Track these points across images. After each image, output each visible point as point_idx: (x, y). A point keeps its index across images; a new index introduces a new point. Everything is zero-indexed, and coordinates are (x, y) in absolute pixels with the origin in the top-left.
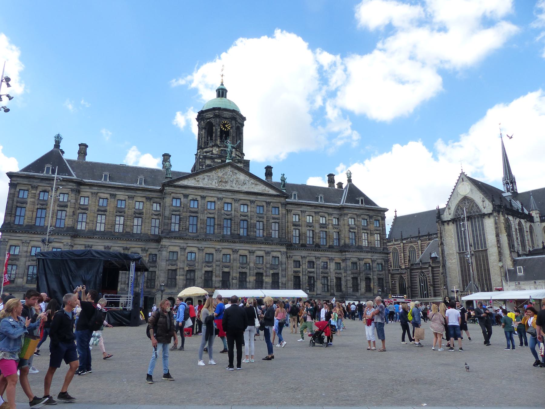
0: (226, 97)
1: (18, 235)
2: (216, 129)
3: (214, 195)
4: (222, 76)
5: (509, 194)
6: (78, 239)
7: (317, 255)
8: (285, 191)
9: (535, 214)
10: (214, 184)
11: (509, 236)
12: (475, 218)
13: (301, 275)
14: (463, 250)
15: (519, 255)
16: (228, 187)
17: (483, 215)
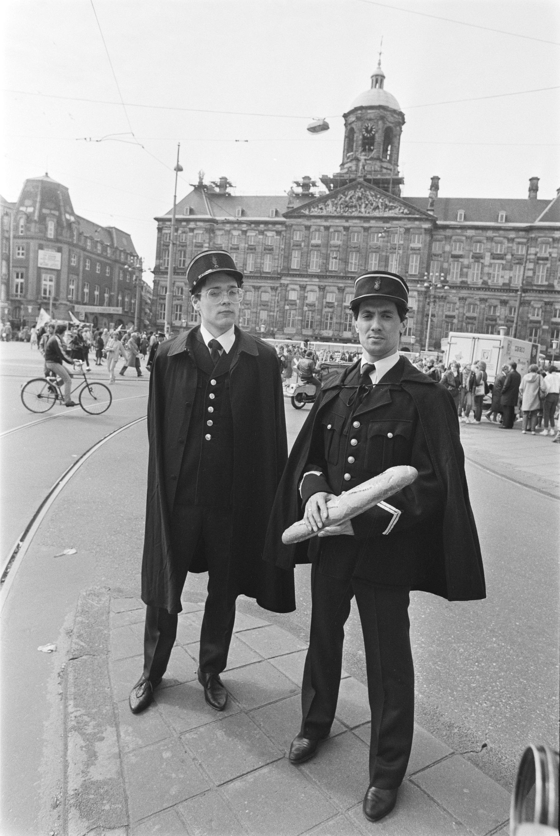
3: (338, 224)
7: (483, 297)
8: (431, 213)
13: (455, 321)
16: (355, 214)
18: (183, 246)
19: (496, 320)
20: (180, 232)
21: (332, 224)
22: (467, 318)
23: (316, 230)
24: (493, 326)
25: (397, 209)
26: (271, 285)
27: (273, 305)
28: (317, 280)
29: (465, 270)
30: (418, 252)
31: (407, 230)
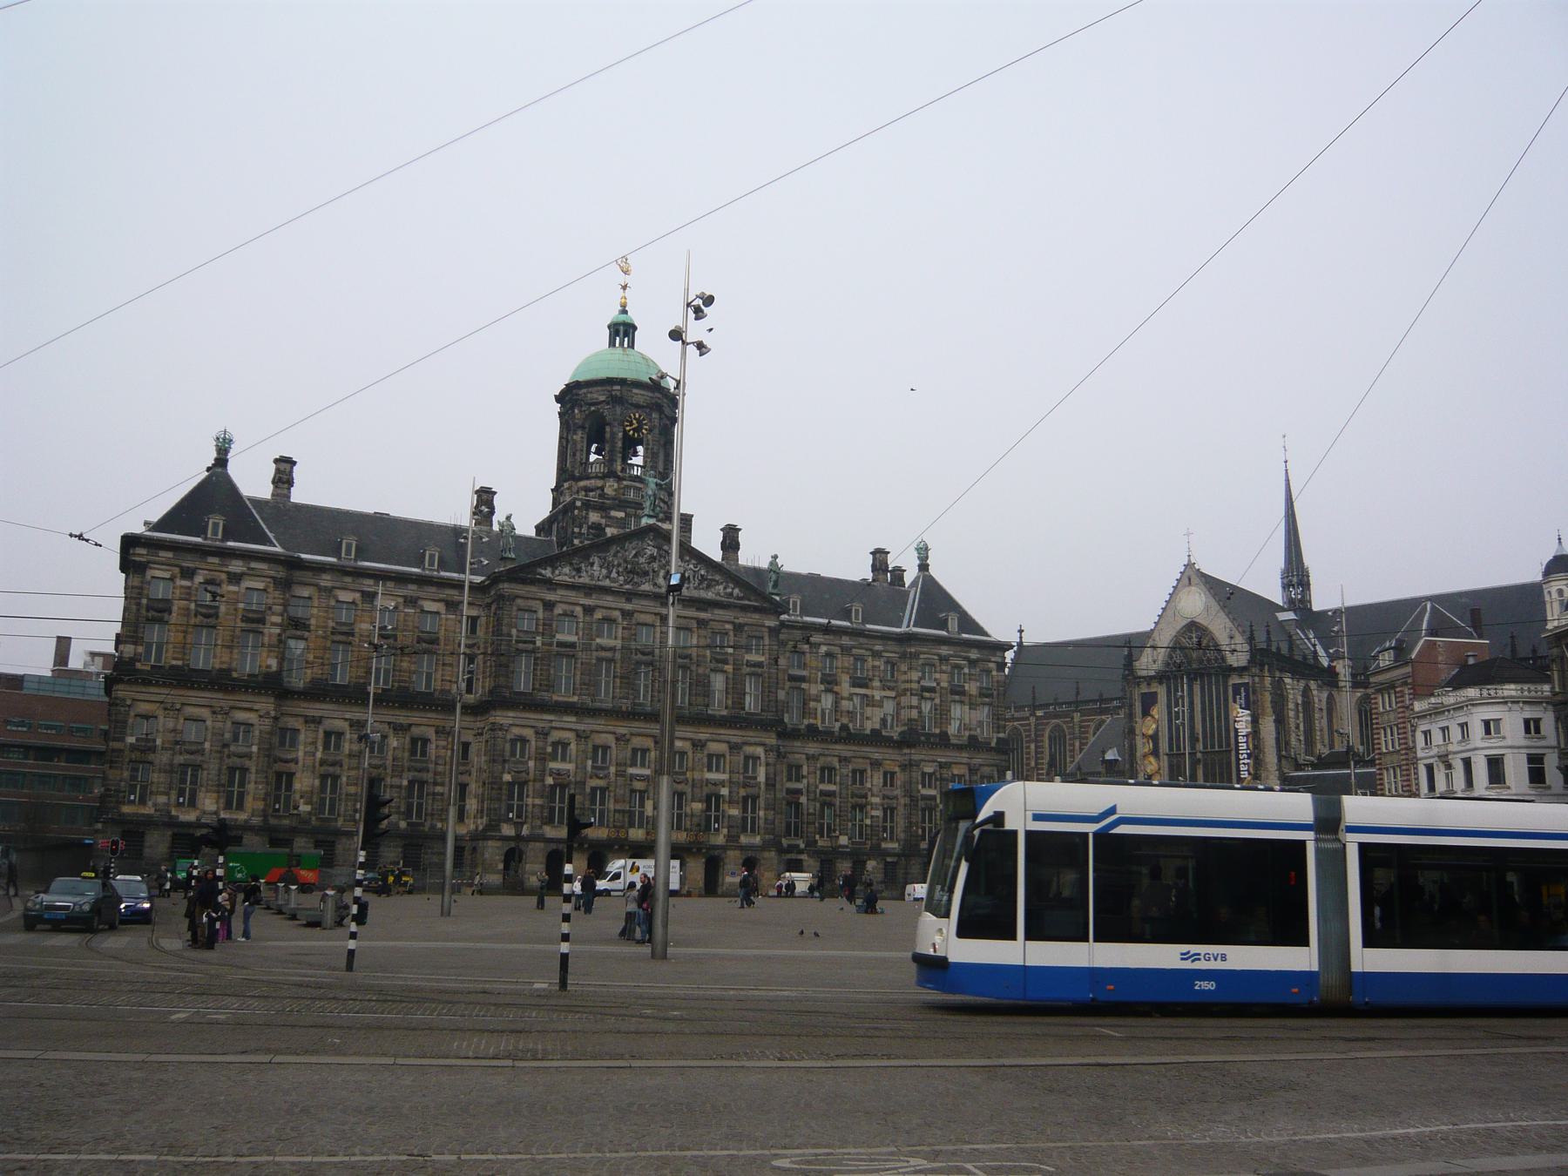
0: (631, 345)
1: (152, 689)
2: (613, 434)
3: (613, 605)
4: (624, 287)
5: (1290, 616)
6: (289, 702)
7: (844, 754)
9: (1343, 669)
10: (618, 581)
11: (1280, 721)
12: (1209, 675)
13: (803, 799)
14: (1178, 748)
15: (1298, 767)
16: (646, 587)
17: (1231, 669)
18: (207, 616)
19: (865, 796)
20: (199, 579)
21: (600, 603)
22: (823, 793)
23: (565, 614)
24: (862, 807)
25: (721, 587)
26: (438, 723)
27: (440, 768)
28: (574, 719)
29: (812, 704)
30: (759, 670)
31: (738, 628)
